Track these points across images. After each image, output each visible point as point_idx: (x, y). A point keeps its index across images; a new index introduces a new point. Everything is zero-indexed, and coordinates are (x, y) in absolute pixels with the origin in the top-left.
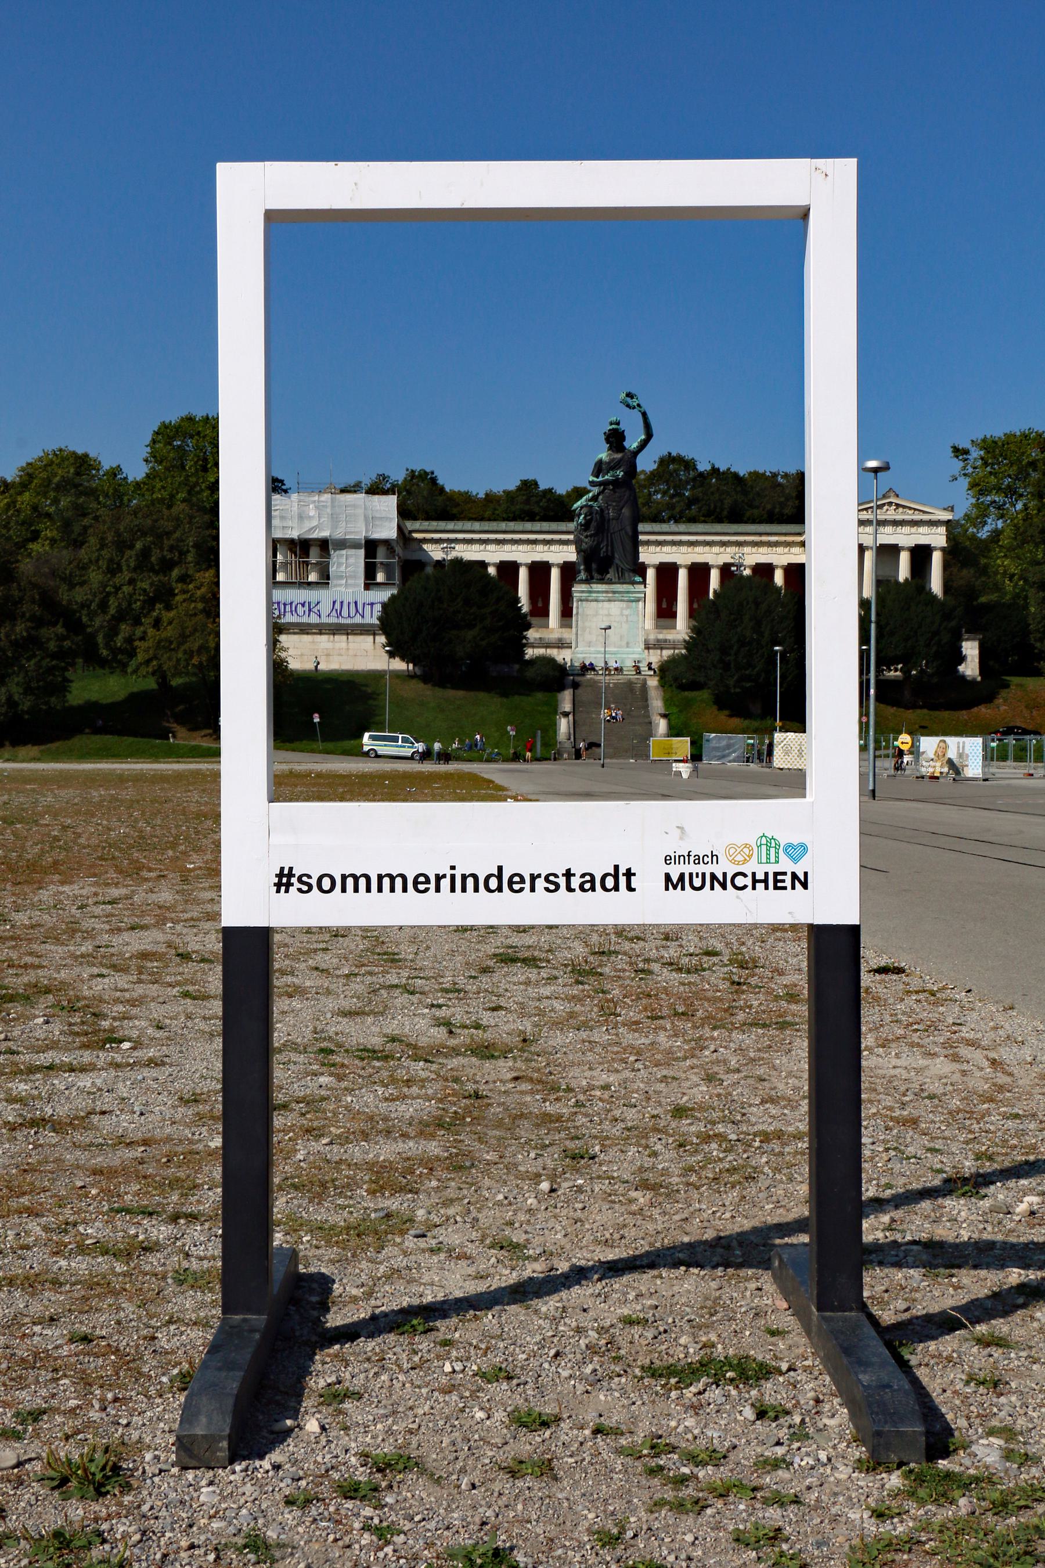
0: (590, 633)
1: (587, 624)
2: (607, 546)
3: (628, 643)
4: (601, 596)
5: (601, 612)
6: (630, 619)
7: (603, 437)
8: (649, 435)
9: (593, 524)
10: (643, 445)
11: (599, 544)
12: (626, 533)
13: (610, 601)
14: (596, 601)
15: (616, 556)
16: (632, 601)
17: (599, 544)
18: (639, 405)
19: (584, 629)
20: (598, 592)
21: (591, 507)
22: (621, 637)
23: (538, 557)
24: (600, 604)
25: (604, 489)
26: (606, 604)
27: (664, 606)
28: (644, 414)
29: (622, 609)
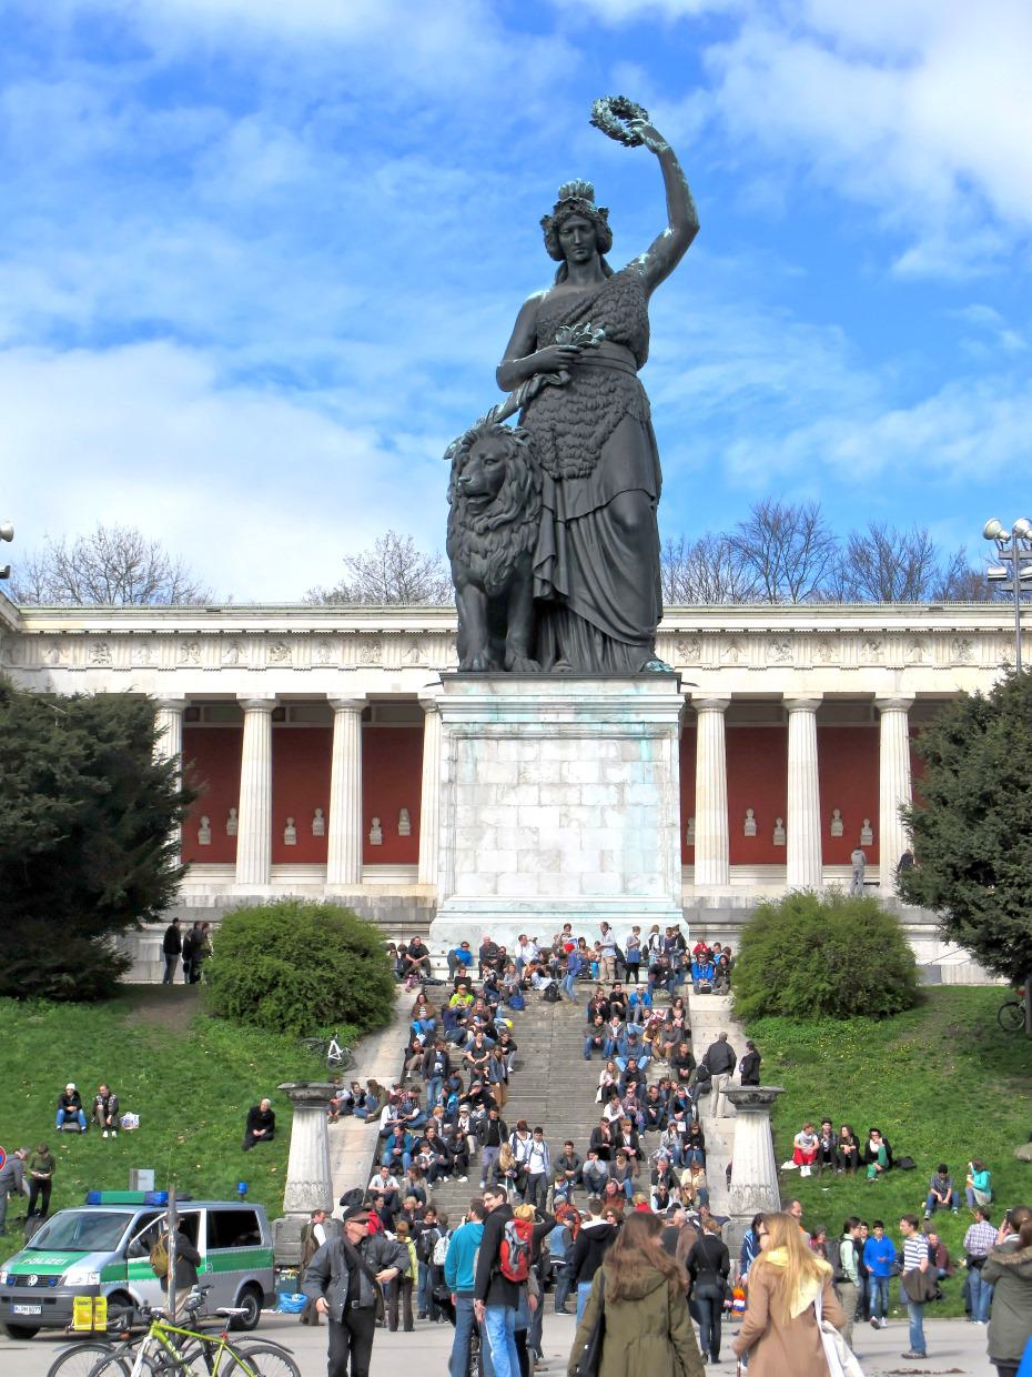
0: (497, 845)
1: (487, 816)
2: (555, 558)
3: (625, 880)
4: (533, 723)
5: (533, 774)
6: (630, 796)
7: (538, 236)
8: (687, 231)
9: (510, 489)
10: (665, 262)
11: (528, 554)
12: (617, 520)
13: (562, 737)
14: (516, 737)
15: (582, 592)
16: (637, 738)
17: (528, 554)
18: (651, 132)
19: (477, 829)
20: (523, 708)
21: (502, 434)
22: (603, 856)
23: (384, 684)
24: (530, 751)
25: (541, 390)
26: (550, 749)
27: (750, 826)
28: (667, 159)
29: (604, 763)
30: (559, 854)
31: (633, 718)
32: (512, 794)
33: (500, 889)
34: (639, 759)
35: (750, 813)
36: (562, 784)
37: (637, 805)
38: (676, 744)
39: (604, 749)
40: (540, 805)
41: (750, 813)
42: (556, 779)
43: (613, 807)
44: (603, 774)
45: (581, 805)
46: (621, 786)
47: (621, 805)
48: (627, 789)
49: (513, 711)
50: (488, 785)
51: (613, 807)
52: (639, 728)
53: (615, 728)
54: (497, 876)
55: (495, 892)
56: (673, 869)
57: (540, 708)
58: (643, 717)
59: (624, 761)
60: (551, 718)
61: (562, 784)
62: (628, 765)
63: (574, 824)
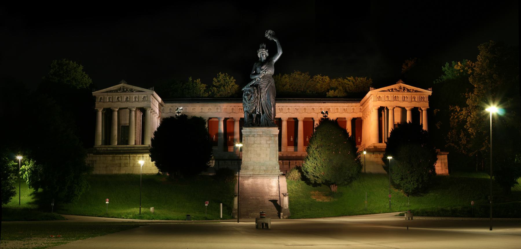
3: (270, 158)
5: (256, 142)
6: (271, 146)
20: (255, 132)
26: (258, 138)
29: (267, 141)
30: (260, 155)
31: (271, 133)
32: (253, 145)
33: (251, 160)
34: (272, 140)
35: (292, 137)
36: (260, 144)
37: (272, 147)
38: (278, 138)
39: (267, 139)
40: (257, 147)
41: (292, 137)
42: (260, 143)
43: (268, 147)
44: (267, 142)
45: (263, 147)
46: (269, 144)
47: (269, 147)
48: (270, 145)
49: (253, 133)
50: (249, 144)
51: (268, 147)
52: (272, 135)
53: (268, 135)
54: (251, 158)
55: (250, 160)
56: (277, 157)
57: (257, 132)
58: (273, 133)
59: (270, 140)
60: (259, 133)
61: (260, 144)
62: (270, 141)
63: (262, 150)
